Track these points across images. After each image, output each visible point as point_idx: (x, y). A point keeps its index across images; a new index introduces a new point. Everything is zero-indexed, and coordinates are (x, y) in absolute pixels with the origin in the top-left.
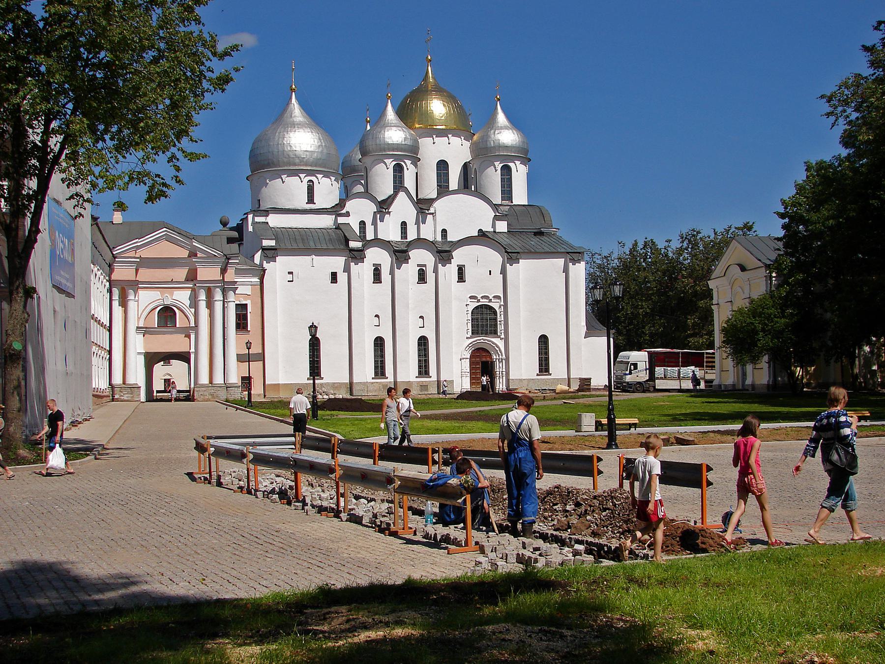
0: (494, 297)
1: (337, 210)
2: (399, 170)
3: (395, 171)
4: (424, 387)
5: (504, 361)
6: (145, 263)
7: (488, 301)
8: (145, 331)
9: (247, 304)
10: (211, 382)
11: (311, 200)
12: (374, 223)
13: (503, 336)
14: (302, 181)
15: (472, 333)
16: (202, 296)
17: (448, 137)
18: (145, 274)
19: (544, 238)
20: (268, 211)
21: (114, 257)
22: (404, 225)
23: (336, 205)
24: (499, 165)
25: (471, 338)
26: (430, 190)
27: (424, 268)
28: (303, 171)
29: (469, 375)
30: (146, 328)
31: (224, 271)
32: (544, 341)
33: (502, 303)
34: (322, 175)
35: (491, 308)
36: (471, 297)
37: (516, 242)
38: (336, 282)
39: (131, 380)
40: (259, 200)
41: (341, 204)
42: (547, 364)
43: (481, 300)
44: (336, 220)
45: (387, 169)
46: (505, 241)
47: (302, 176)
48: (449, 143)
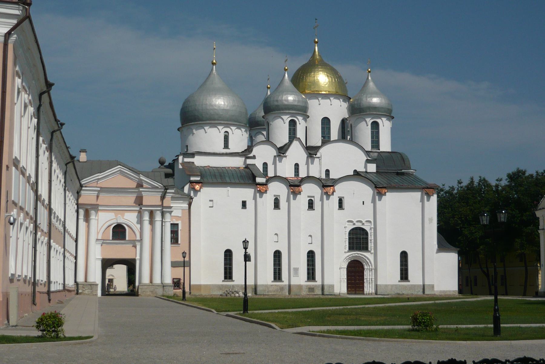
0: (367, 221)
1: (246, 153)
2: (293, 124)
3: (290, 125)
4: (311, 289)
5: (373, 270)
6: (103, 190)
7: (361, 224)
8: (103, 242)
9: (177, 224)
10: (151, 281)
11: (226, 146)
12: (274, 163)
13: (373, 251)
14: (220, 132)
16: (146, 217)
17: (330, 100)
18: (105, 198)
19: (405, 177)
20: (194, 154)
21: (81, 186)
22: (297, 165)
23: (245, 150)
24: (369, 121)
25: (348, 252)
26: (316, 140)
27: (313, 199)
28: (221, 124)
29: (346, 281)
30: (104, 240)
31: (163, 198)
32: (404, 256)
33: (372, 226)
34: (236, 128)
35: (363, 230)
36: (349, 221)
37: (382, 179)
38: (246, 208)
39: (91, 279)
40: (187, 146)
41: (250, 149)
43: (356, 224)
44: (245, 161)
45: (284, 123)
46: (375, 178)
47: (220, 127)
48: (331, 105)
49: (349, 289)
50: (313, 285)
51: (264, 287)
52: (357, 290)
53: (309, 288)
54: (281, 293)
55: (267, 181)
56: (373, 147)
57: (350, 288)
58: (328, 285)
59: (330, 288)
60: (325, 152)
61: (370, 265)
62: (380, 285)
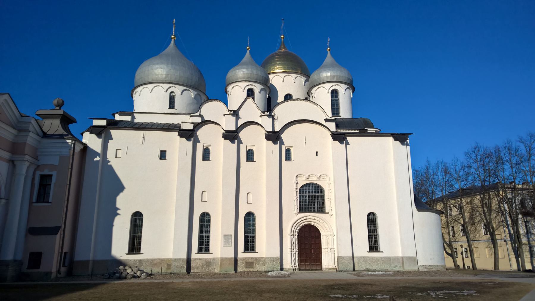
4: (250, 263)
9: (51, 176)
15: (300, 210)
29: (297, 253)
32: (372, 218)
42: (376, 242)
49: (301, 263)
50: (252, 258)
51: (181, 262)
52: (314, 264)
53: (246, 262)
54: (207, 270)
55: (194, 127)
56: (333, 114)
57: (303, 262)
58: (270, 257)
59: (273, 262)
60: (277, 111)
61: (329, 230)
62: (342, 258)
